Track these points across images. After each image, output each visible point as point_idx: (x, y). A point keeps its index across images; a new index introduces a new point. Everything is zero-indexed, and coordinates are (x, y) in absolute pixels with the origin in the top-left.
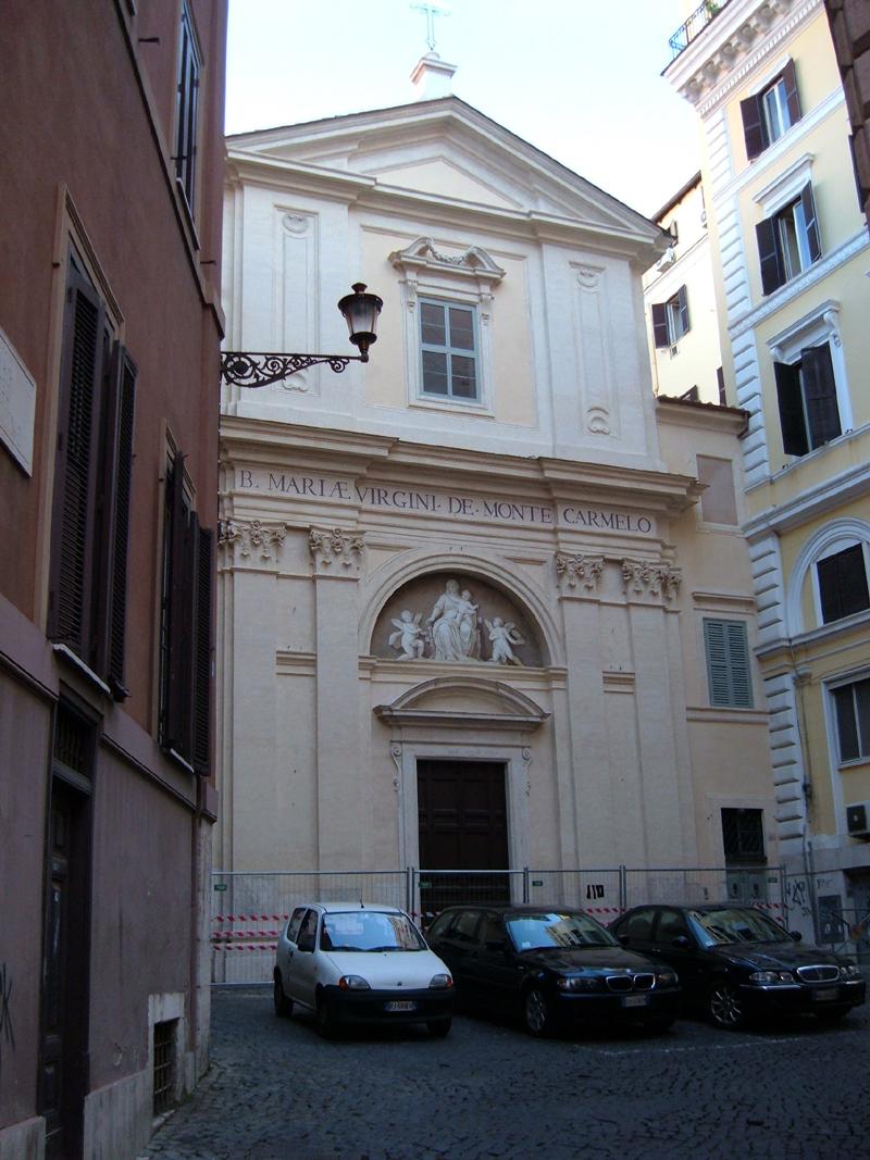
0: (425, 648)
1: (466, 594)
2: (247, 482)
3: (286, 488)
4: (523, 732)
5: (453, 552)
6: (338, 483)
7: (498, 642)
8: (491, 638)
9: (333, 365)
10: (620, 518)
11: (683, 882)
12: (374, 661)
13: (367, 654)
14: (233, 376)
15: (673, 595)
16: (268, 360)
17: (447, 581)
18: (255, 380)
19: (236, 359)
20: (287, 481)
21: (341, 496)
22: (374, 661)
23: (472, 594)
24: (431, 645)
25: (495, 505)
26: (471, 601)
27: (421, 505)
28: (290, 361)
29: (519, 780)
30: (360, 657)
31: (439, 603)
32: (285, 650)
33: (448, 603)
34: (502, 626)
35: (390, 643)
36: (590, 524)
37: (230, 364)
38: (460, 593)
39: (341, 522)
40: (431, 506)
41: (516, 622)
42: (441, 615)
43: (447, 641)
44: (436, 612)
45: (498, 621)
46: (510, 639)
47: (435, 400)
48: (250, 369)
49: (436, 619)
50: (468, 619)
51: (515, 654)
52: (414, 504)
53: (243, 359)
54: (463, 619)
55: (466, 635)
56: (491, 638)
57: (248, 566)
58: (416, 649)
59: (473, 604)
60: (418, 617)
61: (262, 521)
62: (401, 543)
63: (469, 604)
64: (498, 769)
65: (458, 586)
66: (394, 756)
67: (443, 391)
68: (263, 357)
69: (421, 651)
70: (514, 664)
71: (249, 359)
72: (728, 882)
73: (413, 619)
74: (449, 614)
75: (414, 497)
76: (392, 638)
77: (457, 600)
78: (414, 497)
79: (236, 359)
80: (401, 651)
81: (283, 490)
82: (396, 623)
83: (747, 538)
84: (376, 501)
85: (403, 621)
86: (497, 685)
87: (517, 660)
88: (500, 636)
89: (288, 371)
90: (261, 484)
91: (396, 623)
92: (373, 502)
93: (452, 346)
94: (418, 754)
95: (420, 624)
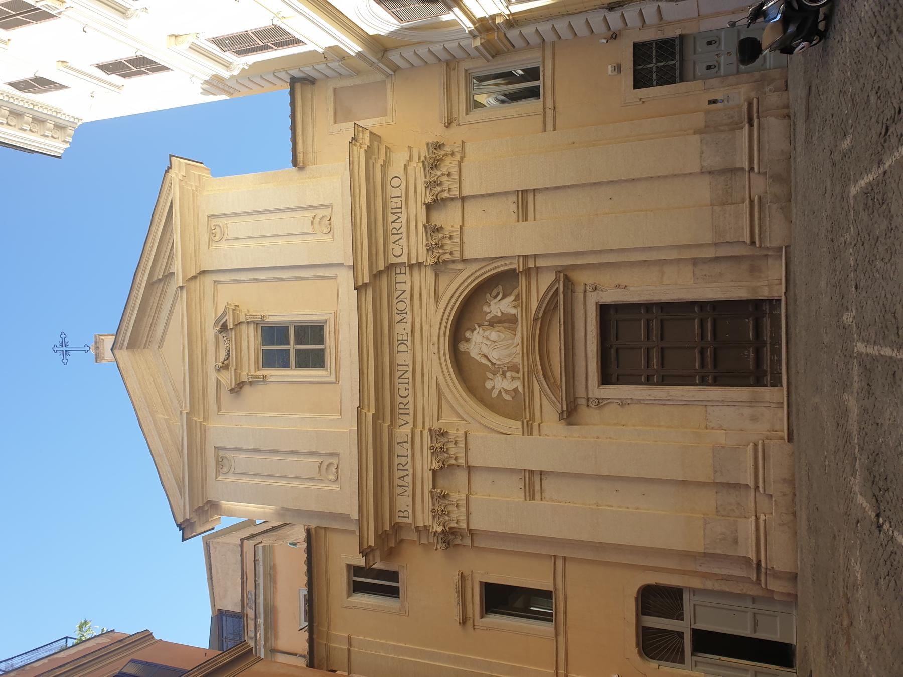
1: (468, 335)
2: (406, 514)
4: (573, 292)
5: (436, 351)
6: (398, 443)
7: (502, 309)
8: (499, 315)
10: (394, 206)
11: (704, 136)
12: (525, 421)
15: (448, 149)
17: (459, 350)
20: (401, 483)
21: (407, 442)
22: (525, 421)
23: (468, 330)
25: (397, 314)
26: (473, 330)
27: (406, 375)
29: (611, 297)
30: (523, 434)
31: (477, 357)
33: (476, 350)
36: (401, 233)
38: (468, 340)
40: (406, 368)
42: (486, 357)
43: (506, 352)
44: (484, 361)
45: (486, 309)
46: (499, 297)
47: (329, 358)
50: (487, 333)
51: (510, 295)
54: (487, 339)
55: (499, 336)
56: (499, 315)
57: (464, 518)
58: (513, 378)
59: (475, 329)
60: (490, 375)
61: (431, 507)
62: (435, 392)
63: (475, 333)
64: (605, 310)
66: (600, 403)
69: (514, 374)
70: (518, 295)
72: (704, 79)
73: (491, 379)
74: (485, 350)
75: (400, 381)
76: (507, 397)
78: (400, 381)
80: (516, 390)
81: (408, 487)
82: (495, 394)
83: (395, 71)
84: (407, 411)
85: (493, 387)
86: (535, 320)
87: (515, 292)
88: (499, 306)
90: (403, 503)
91: (495, 394)
92: (408, 414)
94: (596, 385)
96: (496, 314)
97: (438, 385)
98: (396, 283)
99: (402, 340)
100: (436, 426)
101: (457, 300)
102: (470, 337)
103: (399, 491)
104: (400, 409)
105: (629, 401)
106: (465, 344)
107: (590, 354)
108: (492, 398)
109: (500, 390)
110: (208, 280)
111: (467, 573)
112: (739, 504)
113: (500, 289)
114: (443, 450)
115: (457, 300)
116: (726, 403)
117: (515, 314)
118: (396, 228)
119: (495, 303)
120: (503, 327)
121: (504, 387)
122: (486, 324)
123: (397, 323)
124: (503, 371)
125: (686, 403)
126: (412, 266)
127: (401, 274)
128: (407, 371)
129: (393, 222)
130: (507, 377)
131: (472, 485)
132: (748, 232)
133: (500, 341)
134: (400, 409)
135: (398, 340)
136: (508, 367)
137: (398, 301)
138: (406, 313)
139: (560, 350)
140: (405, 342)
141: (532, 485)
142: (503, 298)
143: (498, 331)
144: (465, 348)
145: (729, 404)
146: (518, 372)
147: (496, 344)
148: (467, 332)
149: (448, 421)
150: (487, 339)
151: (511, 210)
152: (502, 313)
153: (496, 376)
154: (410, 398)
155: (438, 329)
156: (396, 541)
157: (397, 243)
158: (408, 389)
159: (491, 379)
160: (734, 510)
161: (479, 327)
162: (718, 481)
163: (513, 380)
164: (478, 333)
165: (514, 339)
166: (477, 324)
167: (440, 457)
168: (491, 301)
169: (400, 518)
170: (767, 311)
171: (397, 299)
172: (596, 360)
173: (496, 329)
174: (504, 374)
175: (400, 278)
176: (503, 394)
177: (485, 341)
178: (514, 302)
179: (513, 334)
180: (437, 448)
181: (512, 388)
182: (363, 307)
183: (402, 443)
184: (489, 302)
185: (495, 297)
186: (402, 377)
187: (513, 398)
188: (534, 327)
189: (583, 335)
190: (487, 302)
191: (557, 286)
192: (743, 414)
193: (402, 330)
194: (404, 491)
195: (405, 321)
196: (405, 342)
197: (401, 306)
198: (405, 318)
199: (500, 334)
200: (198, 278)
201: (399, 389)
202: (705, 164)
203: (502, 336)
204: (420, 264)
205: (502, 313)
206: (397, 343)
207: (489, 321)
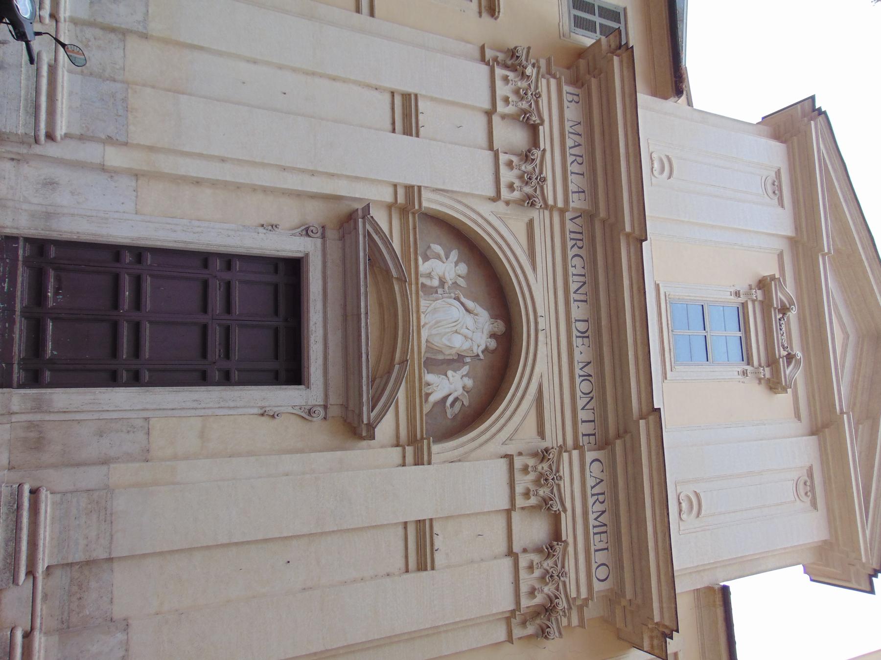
0: (432, 287)
1: (493, 344)
5: (540, 320)
8: (450, 373)
23: (493, 351)
24: (435, 295)
25: (590, 376)
26: (486, 350)
31: (479, 310)
34: (464, 388)
35: (432, 245)
38: (493, 336)
41: (469, 406)
42: (467, 310)
44: (470, 304)
46: (450, 400)
50: (467, 345)
51: (436, 404)
55: (449, 340)
56: (450, 373)
58: (429, 276)
59: (483, 352)
63: (483, 347)
65: (499, 334)
73: (459, 276)
74: (469, 320)
76: (437, 248)
80: (426, 258)
85: (456, 264)
96: (454, 374)
97: (534, 268)
98: (593, 421)
99: (583, 337)
101: (514, 395)
102: (489, 339)
103: (580, 129)
104: (581, 240)
106: (496, 329)
109: (447, 259)
111: (486, 17)
113: (450, 413)
115: (514, 395)
117: (428, 373)
118: (600, 502)
119: (456, 391)
120: (444, 354)
121: (440, 263)
122: (468, 360)
123: (590, 362)
124: (443, 288)
127: (589, 435)
129: (603, 512)
132: (42, 511)
133: (449, 332)
134: (581, 240)
135: (588, 337)
136: (437, 292)
137: (591, 395)
139: (367, 313)
140: (579, 334)
142: (445, 398)
143: (451, 348)
146: (423, 285)
147: (454, 329)
148: (494, 348)
150: (466, 337)
151: (440, 537)
152: (446, 376)
153: (453, 281)
154: (570, 254)
155: (539, 352)
156: (577, 67)
158: (572, 267)
159: (459, 276)
161: (478, 355)
163: (430, 273)
164: (479, 346)
165: (428, 336)
166: (480, 359)
168: (462, 394)
169: (577, 94)
170: (16, 367)
171: (592, 398)
173: (454, 351)
174: (442, 283)
176: (442, 254)
177: (469, 334)
178: (430, 391)
179: (429, 342)
181: (430, 261)
182: (643, 385)
183: (579, 192)
184: (466, 394)
185: (456, 399)
187: (429, 247)
188: (405, 352)
189: (330, 336)
190: (467, 392)
191: (373, 415)
192: (72, 193)
193: (582, 352)
194: (573, 127)
196: (579, 334)
199: (449, 345)
202: (120, 636)
203: (445, 341)
205: (446, 376)
207: (465, 364)
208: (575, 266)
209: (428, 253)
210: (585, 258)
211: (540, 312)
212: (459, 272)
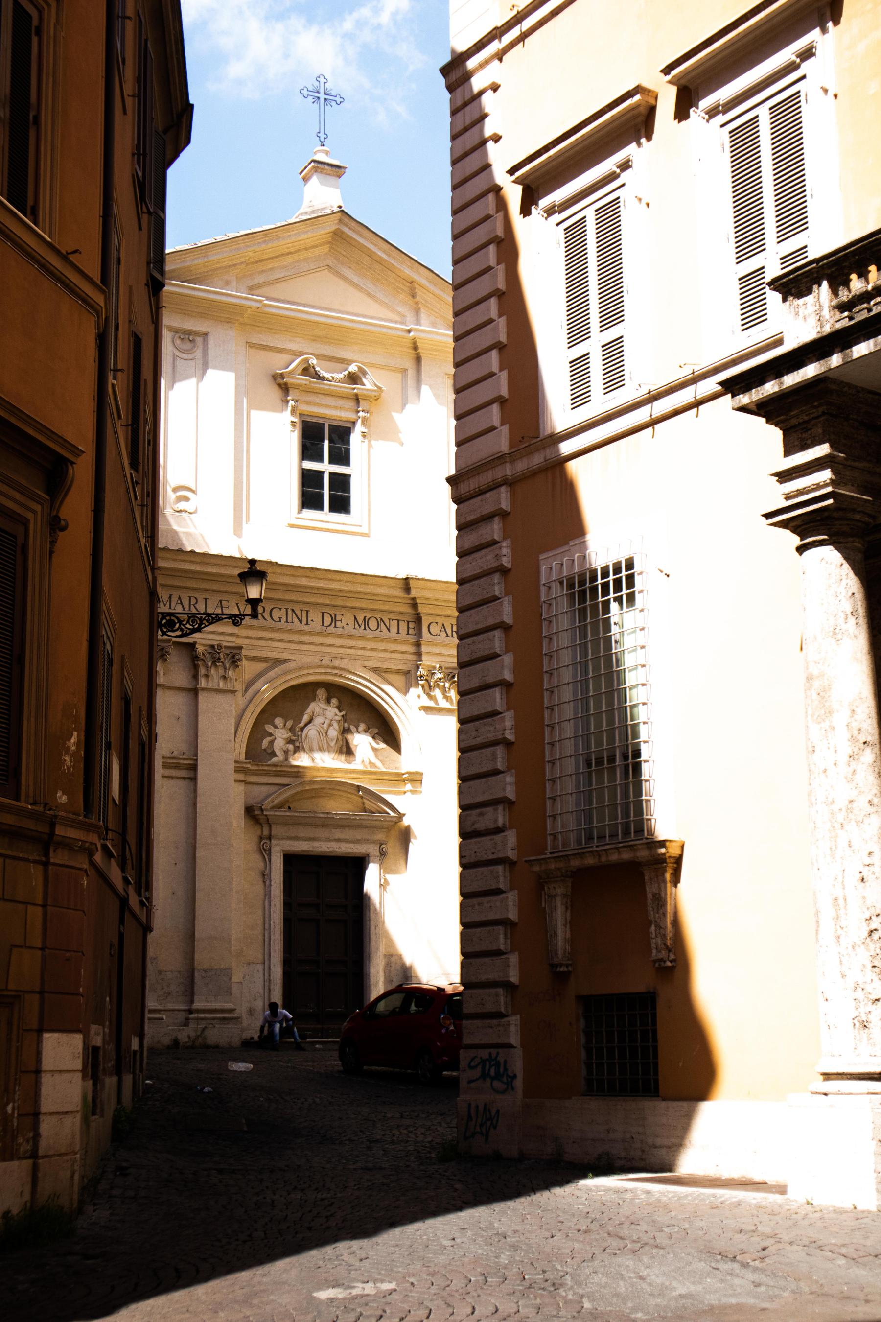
3: (173, 605)
6: (221, 601)
9: (233, 621)
13: (242, 757)
14: (165, 630)
16: (189, 618)
18: (180, 633)
19: (168, 618)
20: (174, 600)
23: (340, 702)
25: (365, 617)
26: (339, 708)
27: (296, 620)
28: (204, 619)
31: (309, 710)
32: (169, 755)
33: (317, 710)
35: (264, 747)
37: (164, 621)
38: (328, 701)
39: (221, 638)
41: (376, 727)
44: (306, 718)
47: (309, 513)
48: (177, 625)
49: (306, 725)
50: (335, 725)
51: (377, 756)
52: (289, 620)
53: (172, 618)
54: (330, 725)
55: (332, 740)
59: (340, 711)
60: (289, 724)
63: (336, 711)
66: (265, 852)
67: (320, 507)
68: (186, 616)
71: (177, 618)
73: (285, 725)
74: (318, 721)
75: (290, 612)
76: (265, 743)
77: (325, 707)
78: (290, 612)
79: (168, 618)
80: (273, 754)
81: (170, 608)
82: (269, 728)
85: (276, 727)
89: (203, 626)
91: (269, 728)
93: (330, 463)
94: (284, 848)
95: (291, 730)
97: (285, 661)
98: (398, 621)
99: (336, 621)
100: (244, 652)
105: (267, 883)
106: (324, 697)
107: (316, 844)
108: (264, 724)
109: (272, 735)
110: (409, 364)
112: (169, 994)
114: (216, 661)
116: (267, 984)
120: (343, 745)
121: (276, 741)
122: (346, 725)
125: (266, 943)
126: (418, 645)
127: (408, 628)
128: (301, 622)
130: (288, 745)
131: (172, 692)
135: (335, 615)
137: (379, 620)
138: (365, 629)
140: (333, 624)
141: (177, 767)
143: (337, 739)
144: (320, 697)
145: (267, 988)
147: (324, 734)
149: (249, 669)
150: (330, 725)
157: (443, 629)
158: (280, 621)
159: (285, 725)
160: (163, 989)
161: (343, 716)
162: (196, 975)
163: (284, 751)
167: (207, 655)
172: (311, 849)
175: (403, 627)
176: (269, 739)
178: (368, 761)
180: (219, 653)
186: (294, 615)
187: (265, 750)
190: (369, 729)
192: (255, 1000)
195: (357, 626)
196: (333, 624)
197: (373, 624)
198: (360, 627)
199: (335, 742)
200: (414, 352)
201: (280, 609)
204: (419, 654)
206: (332, 613)
208: (280, 618)
209: (269, 751)
210: (273, 607)
211: (316, 660)
212: (282, 725)
